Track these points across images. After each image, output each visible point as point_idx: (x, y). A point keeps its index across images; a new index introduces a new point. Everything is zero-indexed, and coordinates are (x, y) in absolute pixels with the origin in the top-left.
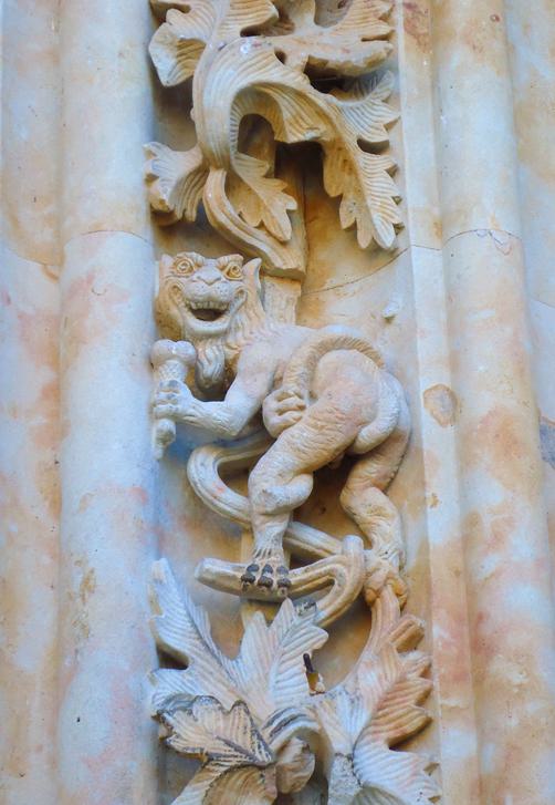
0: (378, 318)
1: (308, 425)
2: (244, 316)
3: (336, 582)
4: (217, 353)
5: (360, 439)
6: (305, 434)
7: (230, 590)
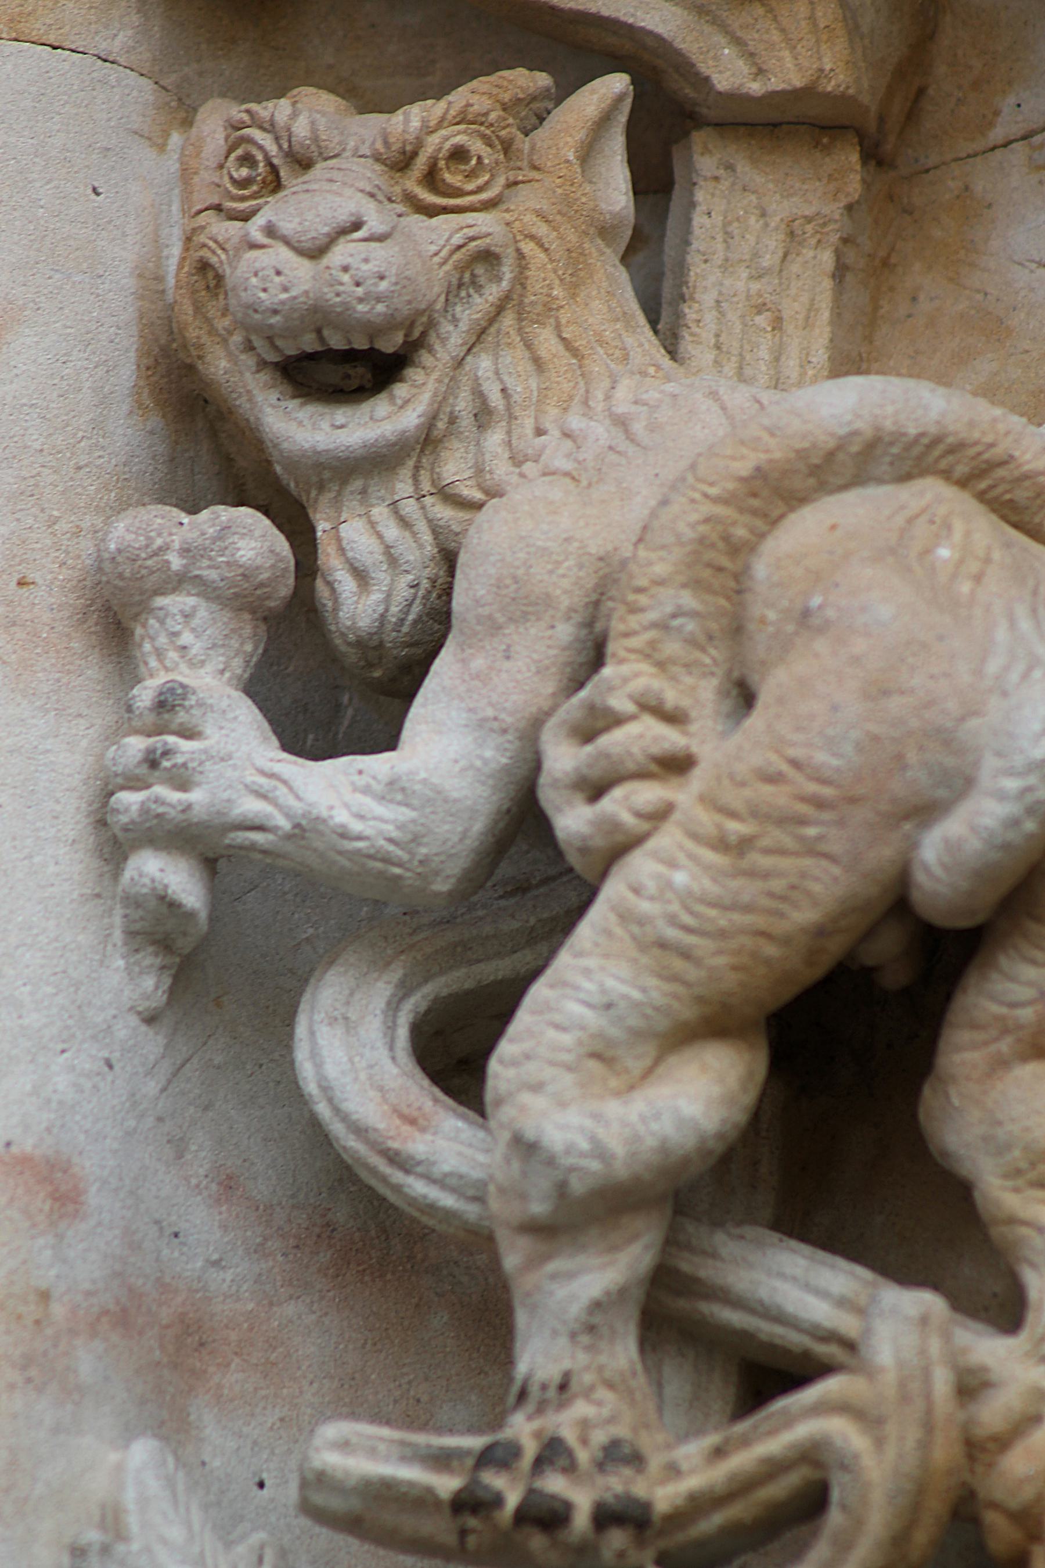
1: (694, 836)
4: (392, 532)
5: (920, 877)
6: (680, 878)
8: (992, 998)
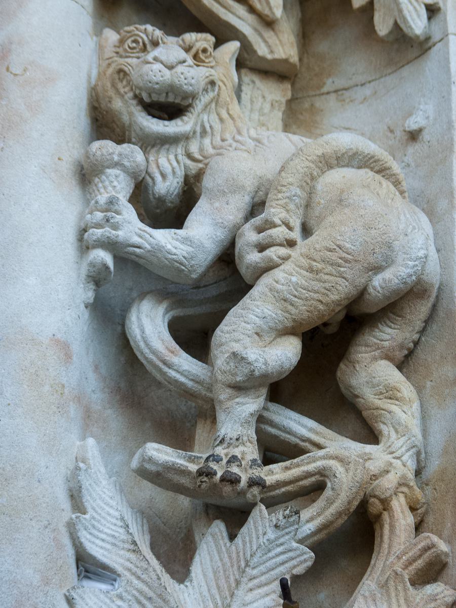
0: (399, 133)
1: (301, 267)
2: (214, 117)
3: (329, 485)
4: (175, 164)
5: (371, 290)
6: (294, 279)
7: (179, 489)
8: (374, 337)
